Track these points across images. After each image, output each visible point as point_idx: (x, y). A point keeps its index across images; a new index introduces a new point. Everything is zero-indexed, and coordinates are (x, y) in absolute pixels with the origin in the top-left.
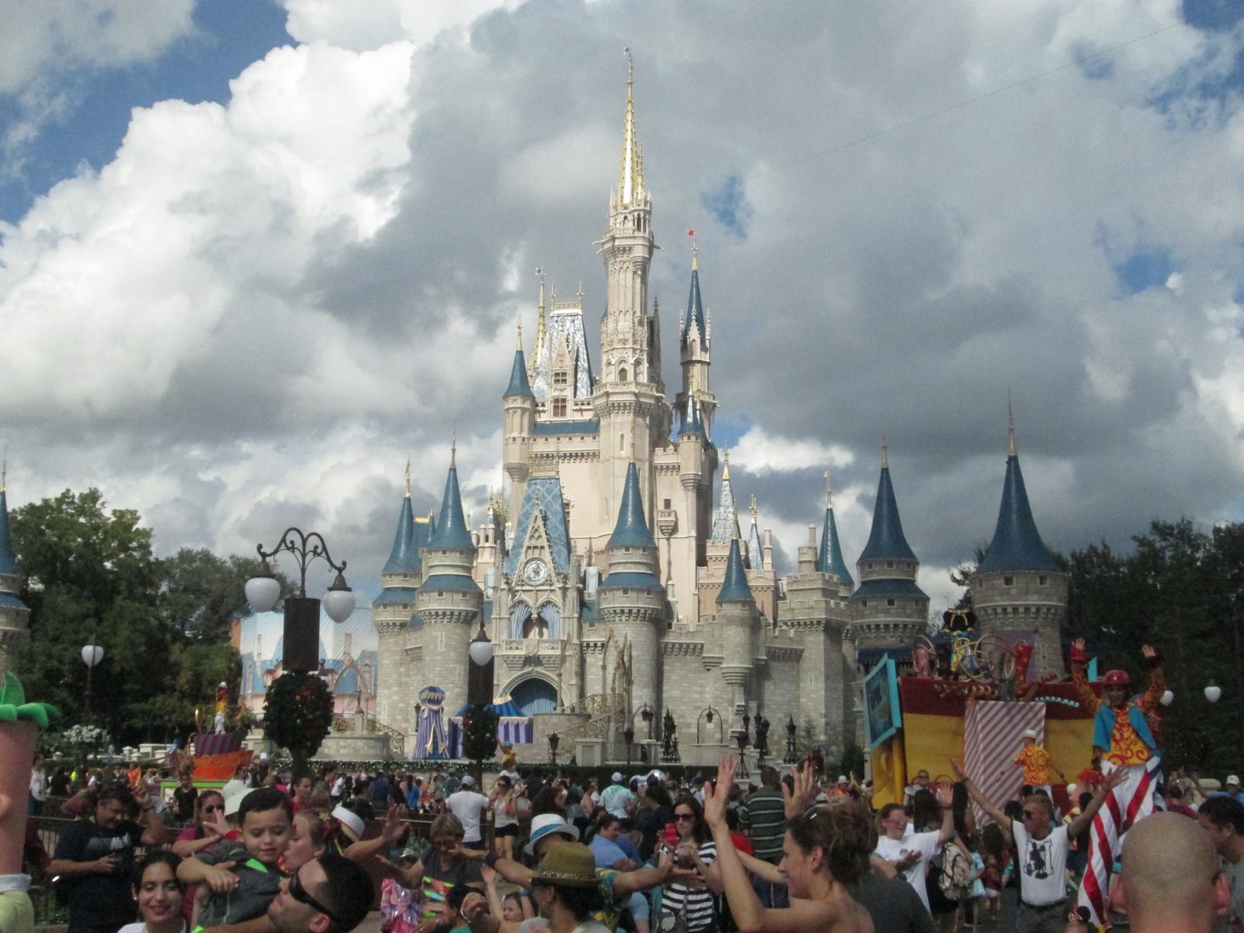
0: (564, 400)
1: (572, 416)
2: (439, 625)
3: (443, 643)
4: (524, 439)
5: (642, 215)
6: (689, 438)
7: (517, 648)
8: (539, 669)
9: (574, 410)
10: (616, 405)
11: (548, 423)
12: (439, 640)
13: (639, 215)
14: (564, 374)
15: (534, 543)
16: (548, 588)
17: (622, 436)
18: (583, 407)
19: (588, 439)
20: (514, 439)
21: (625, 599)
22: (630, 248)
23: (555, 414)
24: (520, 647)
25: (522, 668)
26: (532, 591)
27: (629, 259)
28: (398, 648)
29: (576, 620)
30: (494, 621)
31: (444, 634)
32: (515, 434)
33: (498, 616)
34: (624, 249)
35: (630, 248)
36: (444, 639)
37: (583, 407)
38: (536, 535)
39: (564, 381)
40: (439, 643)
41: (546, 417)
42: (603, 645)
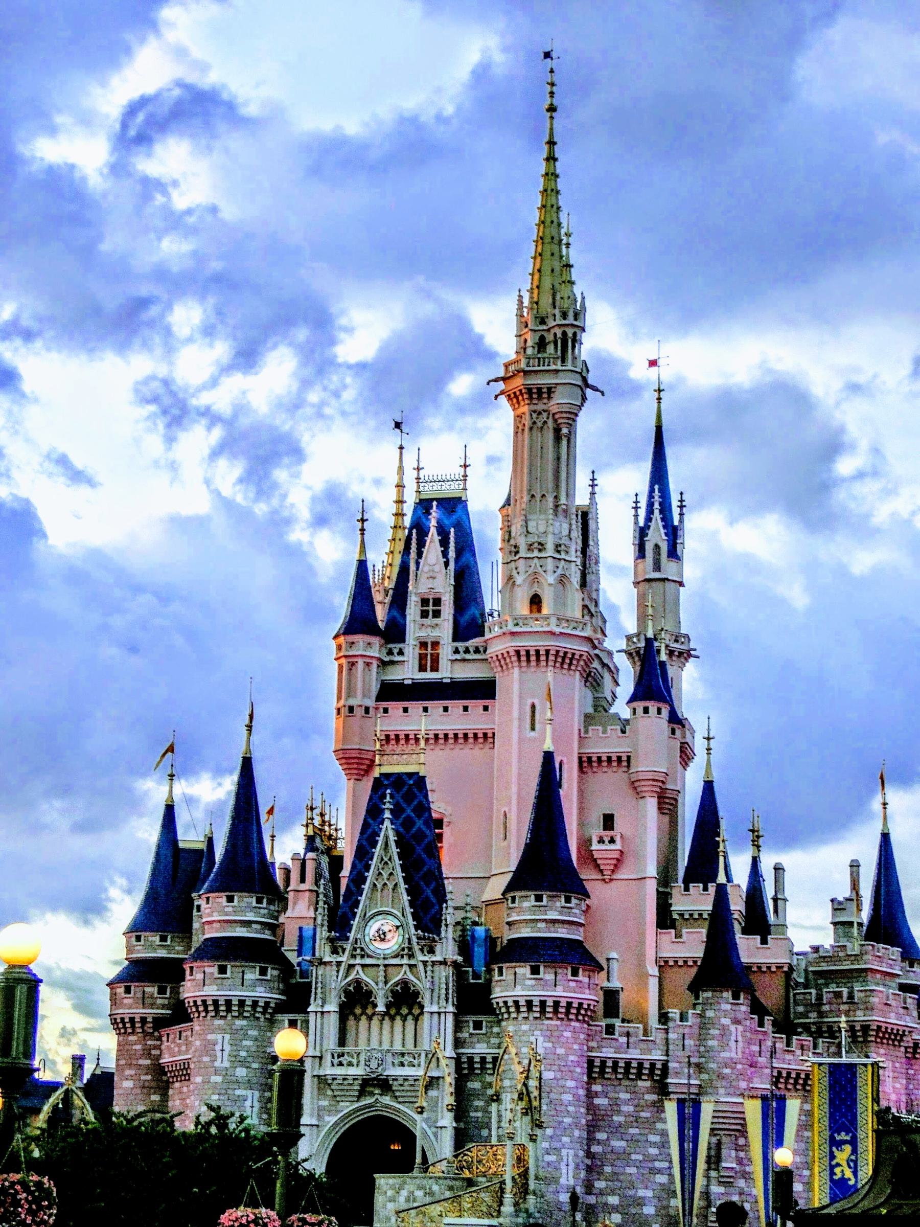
0: (435, 644)
1: (446, 672)
2: (218, 1022)
3: (226, 1054)
4: (367, 710)
5: (570, 333)
6: (646, 711)
7: (350, 1064)
8: (387, 1100)
9: (452, 661)
10: (523, 653)
11: (410, 682)
12: (218, 1048)
13: (564, 334)
14: (437, 602)
16: (405, 961)
17: (533, 707)
18: (468, 656)
19: (476, 705)
21: (533, 982)
23: (422, 668)
24: (355, 1062)
25: (359, 1098)
26: (378, 965)
27: (545, 407)
28: (148, 1062)
29: (450, 1019)
30: (312, 1017)
31: (227, 1037)
32: (352, 702)
34: (540, 390)
35: (550, 391)
36: (227, 1048)
37: (468, 656)
40: (219, 1054)
42: (495, 1060)
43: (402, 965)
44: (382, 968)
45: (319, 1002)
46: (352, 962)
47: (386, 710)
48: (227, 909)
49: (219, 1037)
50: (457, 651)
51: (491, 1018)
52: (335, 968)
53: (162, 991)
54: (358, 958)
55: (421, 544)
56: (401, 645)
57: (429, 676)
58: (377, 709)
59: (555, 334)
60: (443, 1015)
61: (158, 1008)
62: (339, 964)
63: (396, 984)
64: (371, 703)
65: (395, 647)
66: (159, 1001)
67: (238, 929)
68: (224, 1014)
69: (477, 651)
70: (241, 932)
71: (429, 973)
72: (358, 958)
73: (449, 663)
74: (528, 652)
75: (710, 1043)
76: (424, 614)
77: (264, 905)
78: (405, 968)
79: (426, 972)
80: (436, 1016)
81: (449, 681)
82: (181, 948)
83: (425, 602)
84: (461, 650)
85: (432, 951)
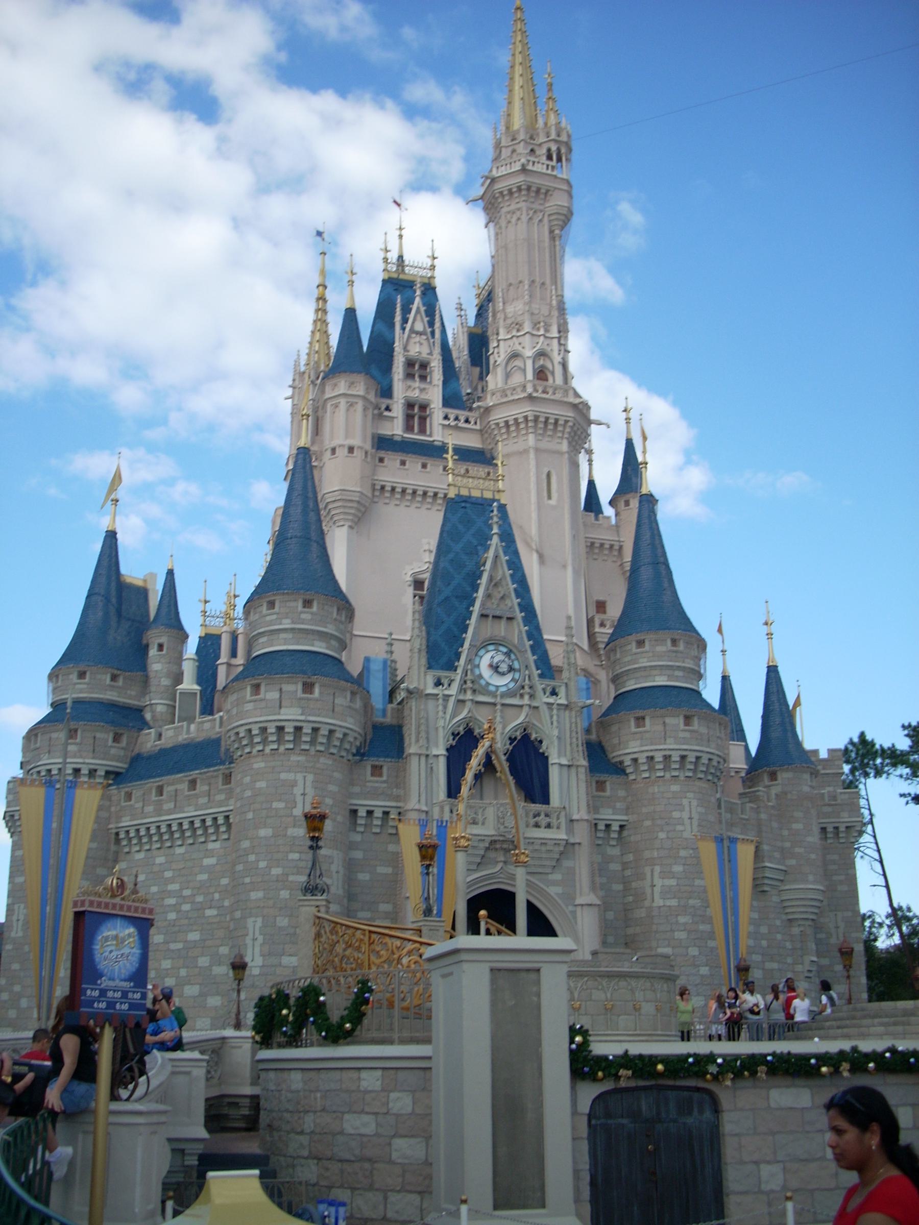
0: (424, 407)
4: (366, 453)
5: (563, 151)
9: (444, 425)
12: (298, 791)
14: (424, 366)
15: (493, 608)
17: (549, 475)
18: (462, 424)
19: (479, 470)
20: (351, 449)
21: (687, 735)
22: (547, 191)
23: (409, 428)
26: (494, 704)
27: (542, 207)
31: (310, 778)
33: (424, 752)
35: (547, 191)
36: (310, 791)
38: (497, 595)
39: (423, 378)
41: (396, 428)
43: (521, 706)
44: (499, 707)
45: (422, 742)
46: (461, 697)
47: (381, 460)
48: (303, 616)
49: (299, 777)
50: (446, 417)
51: (622, 778)
52: (441, 701)
53: (117, 738)
54: (469, 692)
55: (406, 310)
56: (388, 401)
57: (415, 437)
58: (373, 457)
59: (549, 150)
60: (573, 770)
61: (111, 760)
62: (447, 697)
63: (516, 729)
64: (368, 446)
65: (384, 402)
66: (113, 751)
67: (316, 643)
68: (307, 747)
69: (467, 421)
70: (319, 647)
71: (555, 718)
72: (469, 692)
73: (440, 427)
74: (547, 419)
75: (795, 826)
76: (409, 376)
77: (343, 619)
78: (526, 709)
79: (552, 717)
80: (566, 769)
81: (440, 444)
82: (133, 693)
83: (410, 363)
84: (452, 417)
85: (554, 693)
